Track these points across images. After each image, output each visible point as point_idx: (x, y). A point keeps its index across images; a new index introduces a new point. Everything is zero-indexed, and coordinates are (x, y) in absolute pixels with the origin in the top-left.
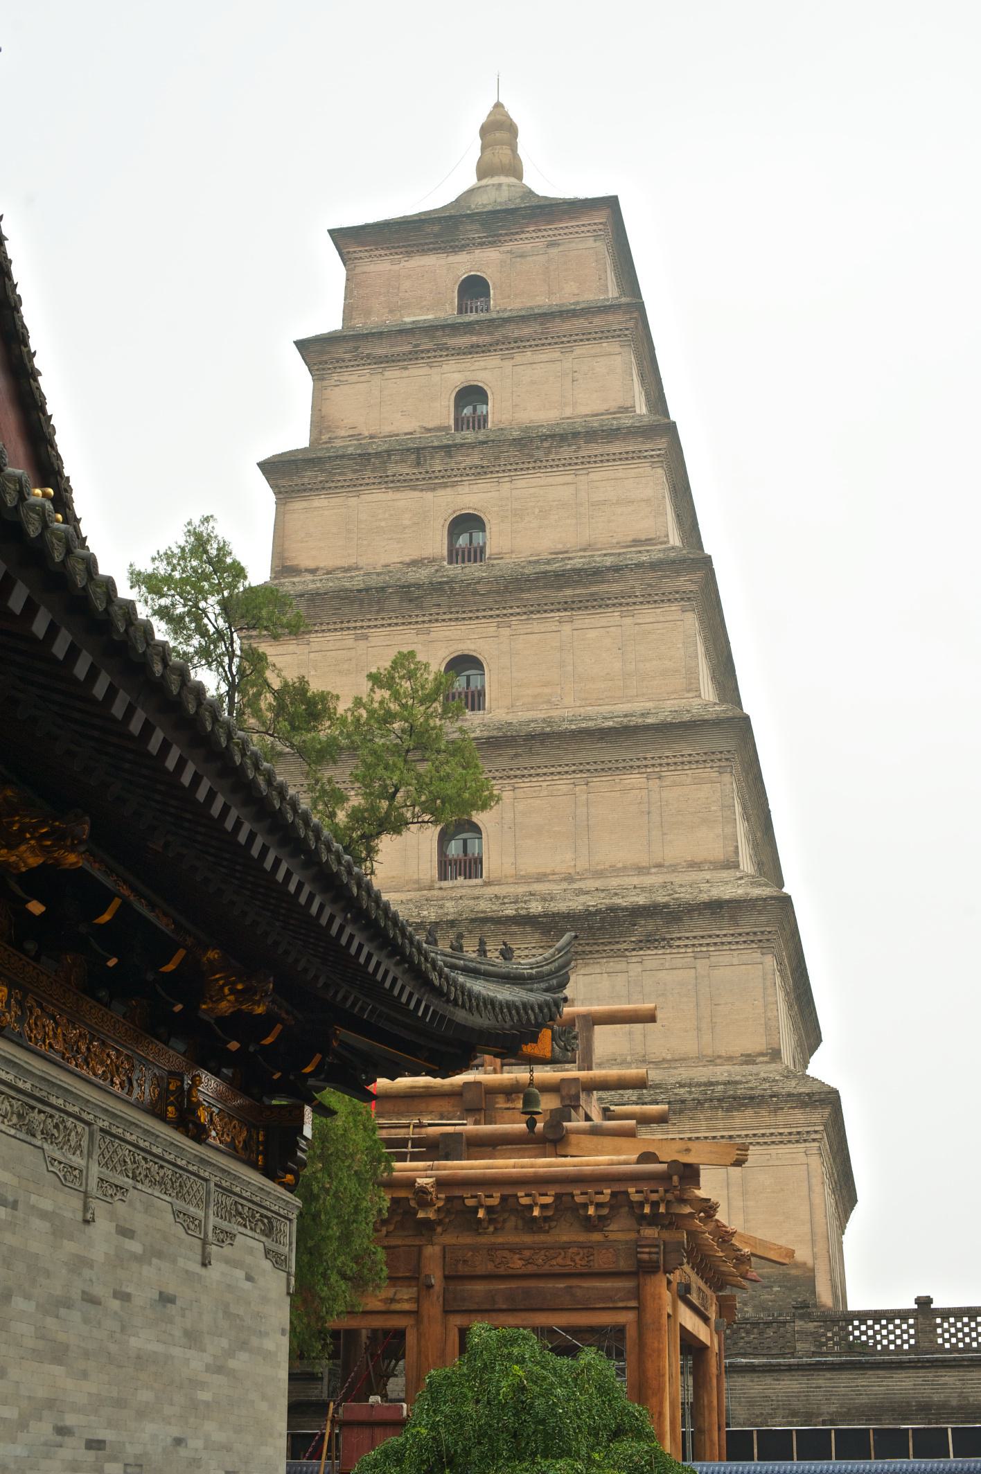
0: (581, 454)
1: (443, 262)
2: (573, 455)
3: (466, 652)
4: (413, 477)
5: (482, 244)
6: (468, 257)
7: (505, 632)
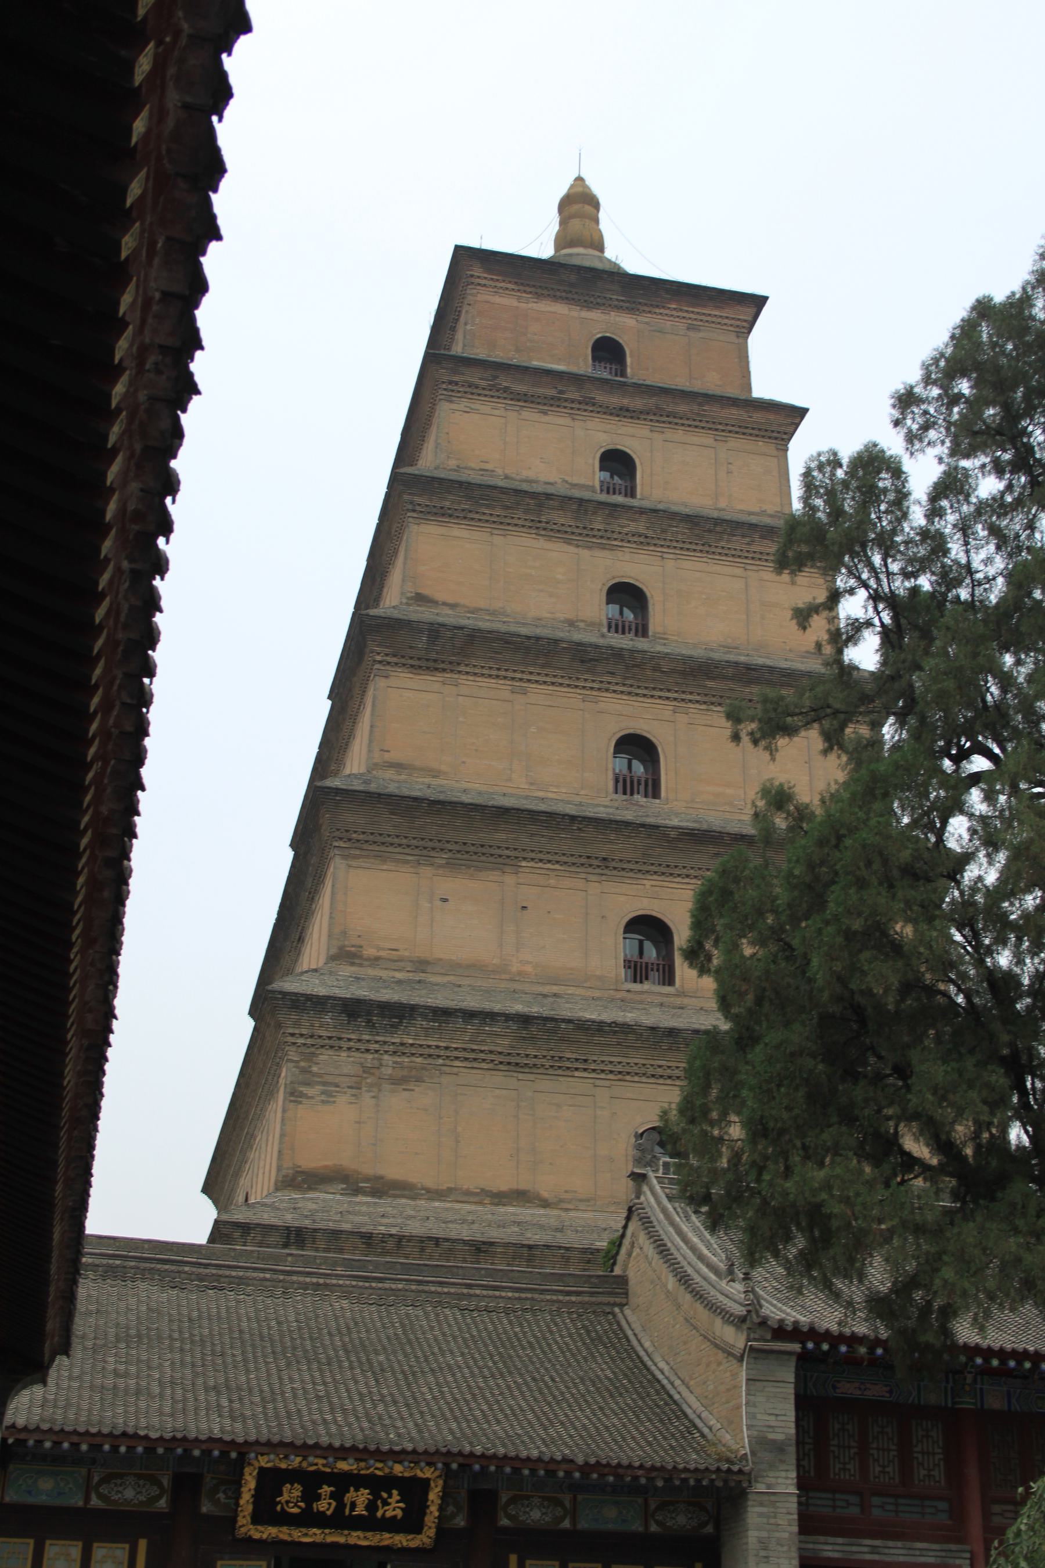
0: (754, 548)
1: (575, 314)
2: (745, 547)
3: (638, 732)
4: (569, 529)
5: (618, 308)
6: (603, 317)
7: (682, 718)
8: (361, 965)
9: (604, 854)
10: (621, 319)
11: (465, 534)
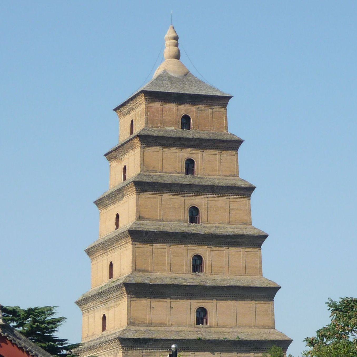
3: (198, 254)
8: (135, 326)
9: (191, 293)
10: (190, 107)
11: (151, 196)
